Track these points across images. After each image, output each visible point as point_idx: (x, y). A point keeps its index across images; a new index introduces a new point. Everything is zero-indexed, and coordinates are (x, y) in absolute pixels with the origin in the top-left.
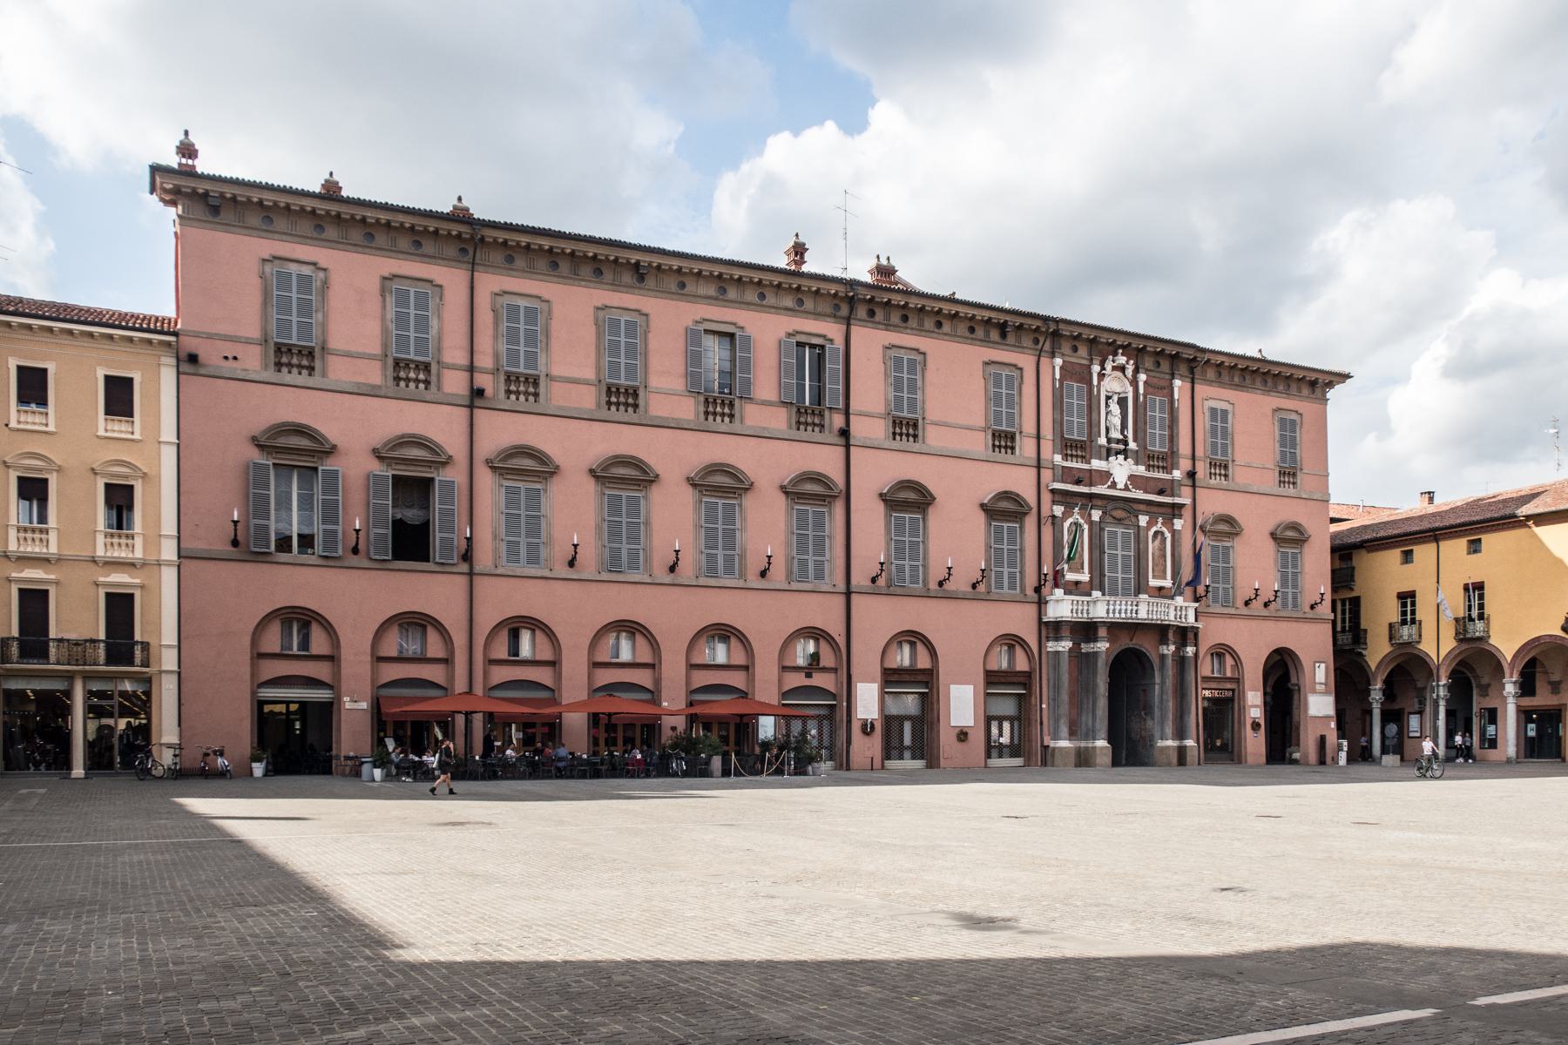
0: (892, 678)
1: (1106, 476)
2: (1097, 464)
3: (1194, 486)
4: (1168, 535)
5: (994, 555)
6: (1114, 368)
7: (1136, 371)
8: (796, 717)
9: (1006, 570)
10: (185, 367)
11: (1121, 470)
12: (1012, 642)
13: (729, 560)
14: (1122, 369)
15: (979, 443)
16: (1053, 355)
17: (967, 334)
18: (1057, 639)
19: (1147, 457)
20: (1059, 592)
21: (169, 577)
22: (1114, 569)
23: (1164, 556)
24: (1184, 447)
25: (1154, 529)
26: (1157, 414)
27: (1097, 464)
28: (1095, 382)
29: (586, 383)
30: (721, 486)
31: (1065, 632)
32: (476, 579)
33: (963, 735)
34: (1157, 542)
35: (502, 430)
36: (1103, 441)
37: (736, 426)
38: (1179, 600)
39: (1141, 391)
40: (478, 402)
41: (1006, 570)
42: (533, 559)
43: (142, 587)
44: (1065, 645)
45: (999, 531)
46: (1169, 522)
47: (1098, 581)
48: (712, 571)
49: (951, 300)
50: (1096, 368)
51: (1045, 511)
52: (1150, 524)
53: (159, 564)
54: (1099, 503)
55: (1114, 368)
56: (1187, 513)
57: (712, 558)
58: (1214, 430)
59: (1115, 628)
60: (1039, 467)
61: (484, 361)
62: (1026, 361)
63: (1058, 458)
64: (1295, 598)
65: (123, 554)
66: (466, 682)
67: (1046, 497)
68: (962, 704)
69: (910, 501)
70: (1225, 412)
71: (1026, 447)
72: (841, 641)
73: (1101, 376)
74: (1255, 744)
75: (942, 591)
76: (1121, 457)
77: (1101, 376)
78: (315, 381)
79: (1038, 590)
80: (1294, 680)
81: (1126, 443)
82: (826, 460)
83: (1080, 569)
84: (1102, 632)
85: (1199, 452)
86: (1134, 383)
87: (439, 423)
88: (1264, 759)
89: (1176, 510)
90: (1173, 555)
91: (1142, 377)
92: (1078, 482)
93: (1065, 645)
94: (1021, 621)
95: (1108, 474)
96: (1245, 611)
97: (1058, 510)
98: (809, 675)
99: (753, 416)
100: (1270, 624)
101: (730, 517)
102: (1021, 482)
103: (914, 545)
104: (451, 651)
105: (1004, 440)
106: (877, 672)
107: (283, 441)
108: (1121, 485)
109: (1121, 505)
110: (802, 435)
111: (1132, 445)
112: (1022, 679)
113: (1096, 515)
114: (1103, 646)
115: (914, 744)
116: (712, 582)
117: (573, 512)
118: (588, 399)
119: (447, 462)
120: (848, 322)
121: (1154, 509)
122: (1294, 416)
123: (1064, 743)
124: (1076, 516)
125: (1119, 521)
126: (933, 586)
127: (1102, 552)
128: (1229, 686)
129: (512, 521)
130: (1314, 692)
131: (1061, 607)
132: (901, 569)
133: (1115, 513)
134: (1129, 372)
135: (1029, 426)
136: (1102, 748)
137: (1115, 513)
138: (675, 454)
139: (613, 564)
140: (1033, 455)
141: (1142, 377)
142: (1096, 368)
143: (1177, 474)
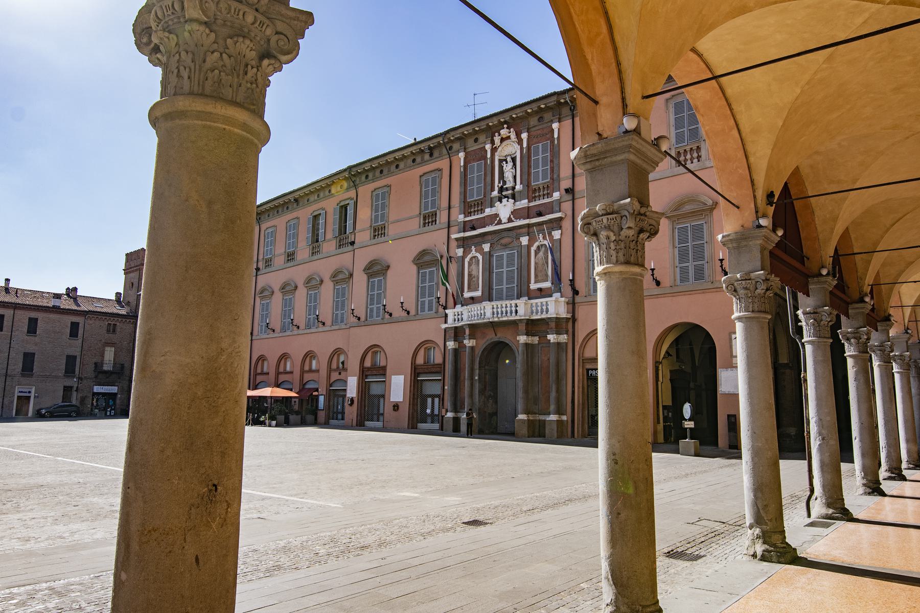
0: (364, 373)
1: (495, 219)
2: (488, 211)
5: (421, 292)
6: (502, 140)
11: (504, 209)
12: (426, 345)
15: (415, 224)
16: (458, 152)
19: (532, 192)
20: (459, 308)
22: (500, 282)
23: (547, 263)
25: (536, 244)
26: (541, 155)
27: (488, 211)
28: (489, 156)
33: (396, 407)
36: (495, 193)
39: (525, 145)
44: (451, 345)
45: (424, 275)
47: (489, 296)
49: (416, 144)
50: (488, 147)
54: (490, 237)
55: (502, 140)
56: (567, 224)
59: (475, 329)
61: (261, 257)
63: (461, 218)
67: (453, 244)
69: (377, 270)
71: (442, 217)
73: (494, 150)
76: (504, 200)
77: (494, 150)
81: (514, 188)
83: (476, 289)
89: (557, 223)
91: (524, 136)
92: (473, 228)
95: (497, 215)
97: (460, 252)
98: (340, 374)
100: (667, 301)
105: (429, 219)
109: (505, 234)
111: (519, 187)
113: (486, 247)
115: (368, 414)
116: (308, 331)
124: (474, 253)
125: (505, 246)
133: (504, 241)
134: (513, 136)
135: (445, 204)
141: (524, 136)
142: (488, 147)
143: (556, 195)
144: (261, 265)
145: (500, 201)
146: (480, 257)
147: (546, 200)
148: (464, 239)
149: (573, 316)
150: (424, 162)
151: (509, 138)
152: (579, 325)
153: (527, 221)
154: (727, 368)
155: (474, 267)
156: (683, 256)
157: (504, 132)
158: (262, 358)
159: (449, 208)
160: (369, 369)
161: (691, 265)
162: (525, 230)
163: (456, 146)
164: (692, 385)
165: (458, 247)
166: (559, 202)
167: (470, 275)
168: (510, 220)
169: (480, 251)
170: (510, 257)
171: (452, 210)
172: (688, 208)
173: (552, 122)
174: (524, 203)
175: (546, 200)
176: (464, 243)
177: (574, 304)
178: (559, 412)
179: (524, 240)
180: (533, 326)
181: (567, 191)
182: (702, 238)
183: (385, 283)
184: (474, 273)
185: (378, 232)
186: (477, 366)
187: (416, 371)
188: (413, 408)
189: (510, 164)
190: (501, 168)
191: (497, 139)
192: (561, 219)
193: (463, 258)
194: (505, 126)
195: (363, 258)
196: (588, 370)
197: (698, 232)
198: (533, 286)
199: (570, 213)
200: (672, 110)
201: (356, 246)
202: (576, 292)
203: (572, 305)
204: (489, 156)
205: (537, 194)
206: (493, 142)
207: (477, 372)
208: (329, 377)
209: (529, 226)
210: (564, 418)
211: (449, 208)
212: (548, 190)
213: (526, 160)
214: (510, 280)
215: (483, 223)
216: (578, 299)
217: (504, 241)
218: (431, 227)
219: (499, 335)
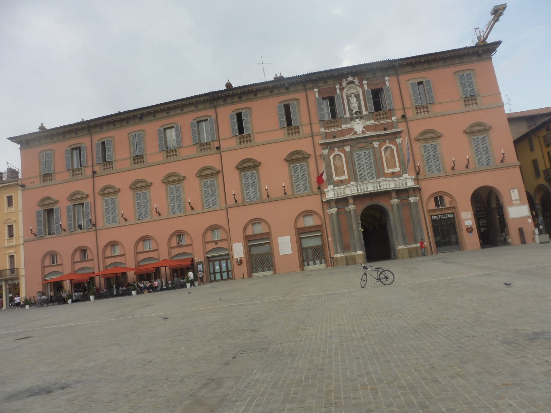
0: (250, 241)
2: (344, 126)
3: (406, 121)
4: (394, 148)
6: (348, 84)
8: (216, 260)
9: (301, 184)
10: (23, 189)
11: (358, 126)
12: (308, 213)
13: (179, 206)
14: (352, 82)
16: (313, 88)
17: (270, 94)
18: (331, 208)
20: (331, 187)
21: (22, 248)
24: (397, 105)
27: (344, 126)
29: (127, 159)
30: (173, 180)
31: (333, 204)
32: (98, 232)
34: (388, 152)
35: (101, 182)
36: (348, 115)
37: (179, 158)
38: (405, 176)
40: (95, 175)
41: (301, 184)
42: (114, 221)
43: (16, 252)
44: (334, 210)
46: (393, 141)
47: (354, 177)
48: (173, 212)
50: (337, 86)
51: (318, 154)
52: (380, 146)
53: (19, 245)
54: (349, 143)
55: (348, 84)
57: (173, 207)
59: (357, 198)
60: (312, 136)
62: (301, 96)
63: (322, 130)
64: (488, 159)
65: (11, 244)
66: (96, 266)
67: (318, 148)
68: (285, 245)
71: (305, 130)
72: (227, 228)
73: (342, 89)
74: (472, 240)
75: (269, 199)
76: (357, 120)
77: (342, 89)
78: (53, 182)
79: (319, 188)
80: (501, 201)
81: (361, 112)
82: (212, 161)
84: (351, 201)
85: (407, 104)
86: (362, 86)
87: (84, 186)
88: (479, 246)
90: (398, 156)
92: (335, 137)
93: (334, 210)
94: (313, 203)
95: (352, 129)
96: (453, 172)
97: (326, 152)
99: (183, 153)
101: (178, 191)
102: (303, 144)
103: (254, 184)
104: (93, 256)
106: (241, 237)
107: (46, 202)
108: (360, 132)
110: (203, 153)
111: (364, 113)
112: (318, 229)
114: (352, 207)
117: (126, 202)
118: (128, 164)
119: (87, 196)
120: (215, 107)
121: (384, 138)
123: (340, 255)
125: (362, 148)
126: (265, 197)
127: (353, 164)
128: (449, 212)
129: (107, 210)
130: (512, 205)
131: (331, 193)
132: (248, 194)
134: (357, 82)
136: (360, 255)
137: (358, 145)
138: (154, 174)
139: (140, 217)
140: (310, 132)
141: (365, 82)
142: (337, 86)
143: (394, 118)
144: (97, 169)
146: (343, 155)
147: (386, 121)
150: (280, 94)
151: (352, 82)
152: (423, 192)
155: (337, 161)
157: (350, 79)
158: (113, 244)
165: (324, 149)
166: (397, 122)
167: (335, 166)
168: (363, 132)
173: (384, 76)
174: (372, 122)
175: (386, 121)
182: (486, 143)
183: (258, 175)
184: (339, 164)
189: (355, 99)
190: (348, 100)
191: (344, 84)
192: (400, 132)
196: (431, 216)
198: (387, 171)
202: (418, 174)
203: (417, 180)
206: (341, 85)
208: (204, 248)
209: (378, 136)
211: (311, 124)
214: (368, 168)
216: (420, 177)
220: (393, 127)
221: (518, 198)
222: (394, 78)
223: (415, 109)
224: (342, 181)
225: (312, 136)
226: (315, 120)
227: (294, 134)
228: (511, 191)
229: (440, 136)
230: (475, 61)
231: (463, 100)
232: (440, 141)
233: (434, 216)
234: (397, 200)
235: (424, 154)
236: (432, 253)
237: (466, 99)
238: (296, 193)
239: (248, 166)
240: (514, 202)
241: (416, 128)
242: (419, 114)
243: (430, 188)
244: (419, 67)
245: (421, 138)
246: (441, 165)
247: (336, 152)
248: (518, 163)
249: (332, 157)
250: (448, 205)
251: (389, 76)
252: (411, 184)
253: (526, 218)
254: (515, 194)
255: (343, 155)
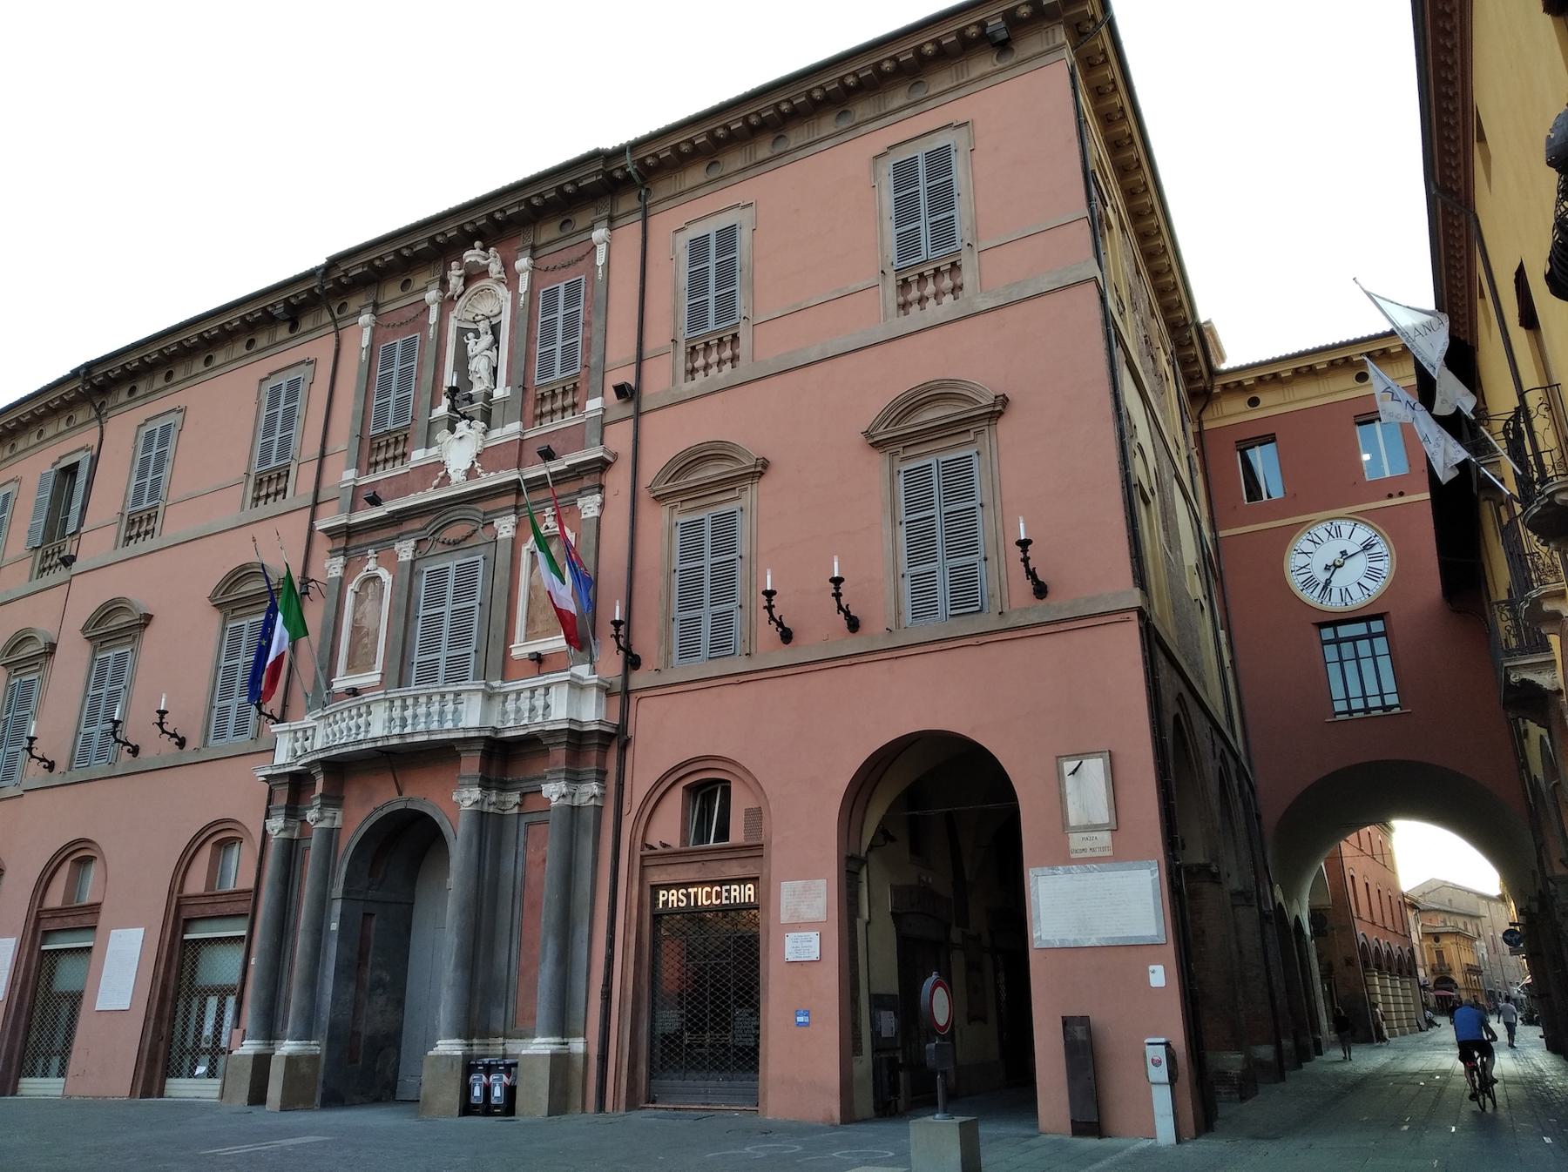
6: (468, 280)
7: (507, 265)
11: (459, 452)
22: (432, 644)
24: (621, 347)
36: (442, 409)
39: (523, 286)
50: (432, 295)
54: (416, 524)
56: (618, 480)
58: (697, 283)
63: (350, 474)
70: (727, 237)
73: (447, 303)
76: (462, 426)
77: (447, 303)
81: (489, 395)
83: (369, 667)
85: (657, 337)
86: (511, 279)
91: (523, 263)
97: (335, 568)
105: (269, 483)
122: (939, 141)
130: (1062, 857)
134: (495, 268)
143: (594, 404)
145: (452, 430)
146: (386, 576)
148: (349, 531)
149: (622, 727)
151: (484, 273)
153: (512, 475)
154: (1053, 864)
155: (368, 606)
156: (920, 545)
157: (471, 256)
159: (323, 455)
160: (55, 913)
161: (941, 569)
162: (510, 500)
163: (353, 304)
164: (956, 935)
165: (333, 553)
167: (356, 629)
168: (470, 474)
169: (391, 562)
170: (466, 572)
171: (328, 461)
172: (930, 415)
173: (591, 228)
175: (570, 420)
176: (347, 538)
177: (626, 693)
178: (562, 1026)
179: (505, 527)
180: (504, 756)
181: (621, 391)
182: (969, 494)
184: (366, 623)
185: (139, 524)
186: (338, 890)
187: (181, 915)
188: (157, 1030)
189: (487, 339)
190: (461, 348)
192: (602, 465)
193: (342, 583)
194: (477, 244)
195: (88, 596)
196: (655, 889)
197: (959, 478)
198: (521, 649)
199: (625, 449)
200: (887, 182)
201: (76, 567)
202: (632, 662)
203: (621, 694)
204: (433, 317)
205: (547, 407)
206: (444, 283)
207: (337, 907)
209: (515, 488)
210: (577, 1046)
212: (569, 395)
213: (524, 323)
214: (460, 635)
215: (401, 486)
216: (638, 679)
217: (453, 533)
218: (272, 507)
219: (406, 795)
220: (582, 446)
221: (1102, 815)
222: (630, 233)
223: (682, 357)
224: (354, 692)
225: (316, 504)
226: (342, 438)
227: (270, 500)
228: (1069, 766)
229: (761, 469)
230: (983, 77)
231: (892, 278)
232: (750, 497)
233: (668, 887)
234: (476, 793)
235: (676, 565)
236: (601, 1106)
237: (912, 276)
238: (211, 742)
239: (116, 628)
240: (1076, 841)
241: (666, 440)
242: (700, 376)
243: (665, 738)
244: (734, 161)
245: (672, 486)
246: (737, 614)
247: (371, 564)
248: (1135, 598)
249: (352, 587)
250: (737, 835)
251: (611, 222)
252: (591, 712)
253: (1125, 954)
254: (1087, 793)
255: (386, 576)
